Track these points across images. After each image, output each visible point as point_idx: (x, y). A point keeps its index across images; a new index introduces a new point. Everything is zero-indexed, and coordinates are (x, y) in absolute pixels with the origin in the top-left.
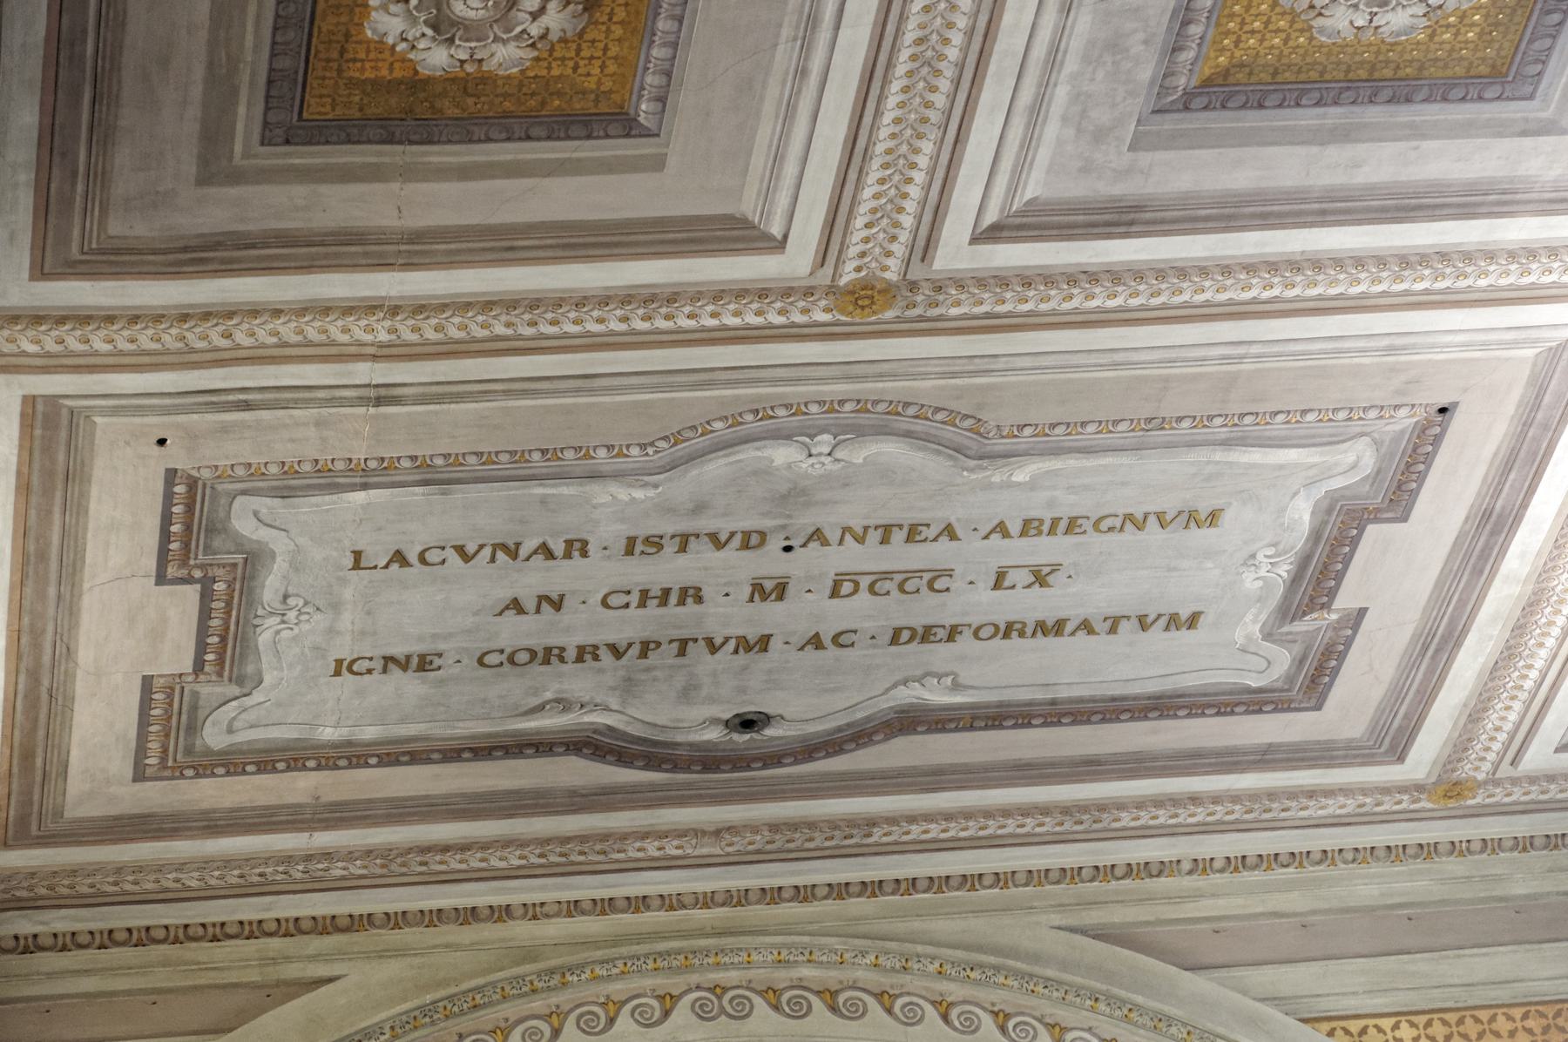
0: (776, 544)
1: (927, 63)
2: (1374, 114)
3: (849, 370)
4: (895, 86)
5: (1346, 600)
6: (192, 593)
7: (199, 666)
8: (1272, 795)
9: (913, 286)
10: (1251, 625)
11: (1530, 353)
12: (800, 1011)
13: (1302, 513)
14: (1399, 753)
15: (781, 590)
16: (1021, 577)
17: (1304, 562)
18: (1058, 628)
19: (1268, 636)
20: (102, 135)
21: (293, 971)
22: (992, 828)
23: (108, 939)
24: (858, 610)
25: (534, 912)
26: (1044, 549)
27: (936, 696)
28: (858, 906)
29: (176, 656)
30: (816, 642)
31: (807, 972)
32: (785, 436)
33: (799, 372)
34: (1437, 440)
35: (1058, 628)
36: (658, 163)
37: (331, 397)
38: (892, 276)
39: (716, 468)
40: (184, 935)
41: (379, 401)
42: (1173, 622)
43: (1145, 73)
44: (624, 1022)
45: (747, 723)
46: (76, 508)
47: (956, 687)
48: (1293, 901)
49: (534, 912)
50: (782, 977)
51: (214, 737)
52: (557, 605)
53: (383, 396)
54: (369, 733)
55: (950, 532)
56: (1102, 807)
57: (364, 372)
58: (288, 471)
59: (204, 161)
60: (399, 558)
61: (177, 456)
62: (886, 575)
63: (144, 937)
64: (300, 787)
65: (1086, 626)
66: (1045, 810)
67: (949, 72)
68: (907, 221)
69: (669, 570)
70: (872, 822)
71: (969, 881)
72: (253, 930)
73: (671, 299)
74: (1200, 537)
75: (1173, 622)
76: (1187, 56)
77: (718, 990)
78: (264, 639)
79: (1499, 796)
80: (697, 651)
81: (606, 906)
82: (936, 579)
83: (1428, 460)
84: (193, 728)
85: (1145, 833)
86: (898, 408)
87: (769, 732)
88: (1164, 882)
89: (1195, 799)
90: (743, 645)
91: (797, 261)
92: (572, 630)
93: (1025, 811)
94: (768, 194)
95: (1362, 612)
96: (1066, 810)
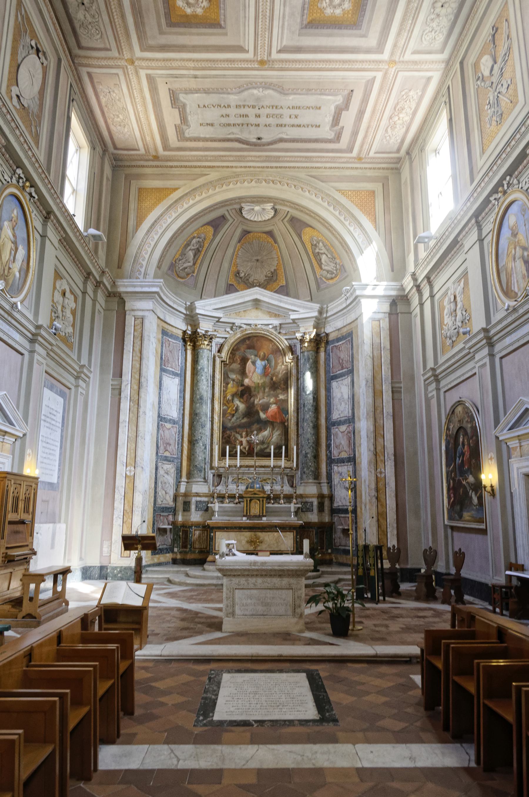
0: (257, 108)
1: (264, 16)
2: (336, 31)
3: (262, 77)
4: (260, 21)
5: (341, 124)
6: (177, 110)
7: (181, 123)
8: (334, 157)
9: (269, 61)
10: (328, 128)
11: (364, 81)
12: (269, 183)
13: (333, 108)
14: (351, 151)
15: (259, 116)
16: (293, 116)
17: (334, 117)
18: (299, 126)
19: (330, 130)
20: (143, 23)
21: (204, 173)
22: (296, 159)
23: (181, 167)
24: (270, 121)
25: (236, 167)
26: (297, 112)
27: (285, 136)
28: (279, 170)
29: (178, 122)
30: (266, 125)
31: (271, 178)
32: (255, 88)
33: (255, 76)
34: (351, 96)
35: (299, 126)
36: (226, 34)
37: (188, 76)
38: (266, 59)
39: (246, 93)
40: (191, 167)
41: (195, 78)
42: (316, 126)
43: (299, 20)
44: (246, 182)
45: (259, 139)
46: (158, 94)
47: (287, 135)
48: (337, 174)
49: (236, 167)
50: (267, 178)
51: (187, 135)
52: (229, 116)
53: (196, 77)
54: (208, 136)
55: (281, 107)
56: (311, 157)
57: (192, 72)
58: (186, 90)
59: (159, 30)
60: (204, 106)
61: (169, 86)
62: (274, 115)
63: (186, 167)
64: (200, 144)
65: (304, 126)
66: (303, 157)
67: (268, 18)
68: (266, 48)
69: (243, 111)
70: (279, 157)
71: (294, 167)
72: (200, 167)
73: (234, 61)
74: (318, 111)
75: (316, 126)
76: (305, 17)
77: (258, 179)
78: (189, 119)
79: (366, 160)
80: (249, 125)
81: (245, 167)
82: (281, 116)
83: (351, 100)
84: (184, 133)
85: (317, 162)
86: (271, 84)
87: (263, 140)
88: (320, 170)
89: (324, 157)
90: (256, 125)
91: (250, 55)
92: (232, 120)
93: (301, 157)
94: (244, 41)
95: (343, 127)
96: (306, 157)
